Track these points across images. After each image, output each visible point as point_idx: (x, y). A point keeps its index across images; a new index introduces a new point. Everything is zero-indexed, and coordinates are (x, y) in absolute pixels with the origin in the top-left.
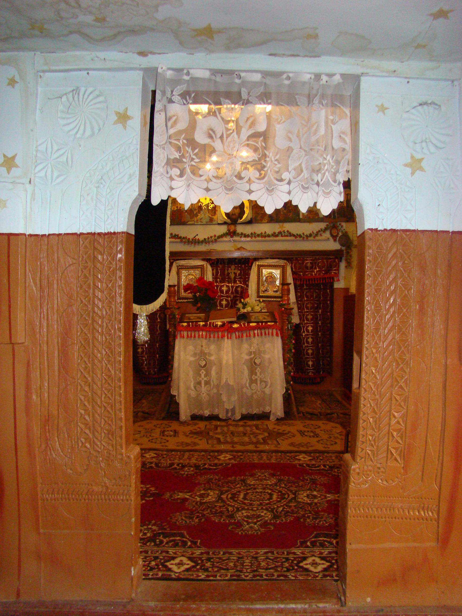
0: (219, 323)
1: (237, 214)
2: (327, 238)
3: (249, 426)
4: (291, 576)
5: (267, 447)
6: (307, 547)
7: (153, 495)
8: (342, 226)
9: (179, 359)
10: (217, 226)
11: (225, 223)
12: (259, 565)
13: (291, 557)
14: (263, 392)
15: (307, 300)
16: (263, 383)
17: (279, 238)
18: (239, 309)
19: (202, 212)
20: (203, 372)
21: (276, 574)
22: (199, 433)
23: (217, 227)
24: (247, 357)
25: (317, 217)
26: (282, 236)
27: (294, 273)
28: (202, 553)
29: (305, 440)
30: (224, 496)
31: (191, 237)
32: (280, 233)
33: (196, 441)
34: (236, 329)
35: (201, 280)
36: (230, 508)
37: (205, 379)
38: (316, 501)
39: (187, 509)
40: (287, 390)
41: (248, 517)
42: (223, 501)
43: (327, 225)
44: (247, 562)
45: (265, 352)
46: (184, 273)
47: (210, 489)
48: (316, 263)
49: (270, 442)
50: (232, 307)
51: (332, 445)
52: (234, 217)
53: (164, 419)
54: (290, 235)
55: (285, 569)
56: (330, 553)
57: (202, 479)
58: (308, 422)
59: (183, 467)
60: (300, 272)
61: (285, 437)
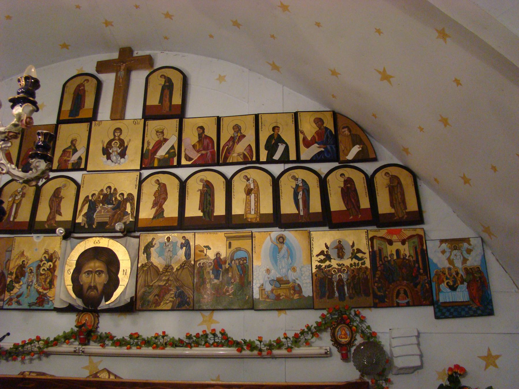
1: (100, 288)
2: (323, 351)
8: (363, 320)
10: (54, 314)
11: (70, 309)
19: (23, 280)
23: (54, 315)
25: (296, 297)
26: (207, 345)
43: (323, 316)
52: (93, 293)
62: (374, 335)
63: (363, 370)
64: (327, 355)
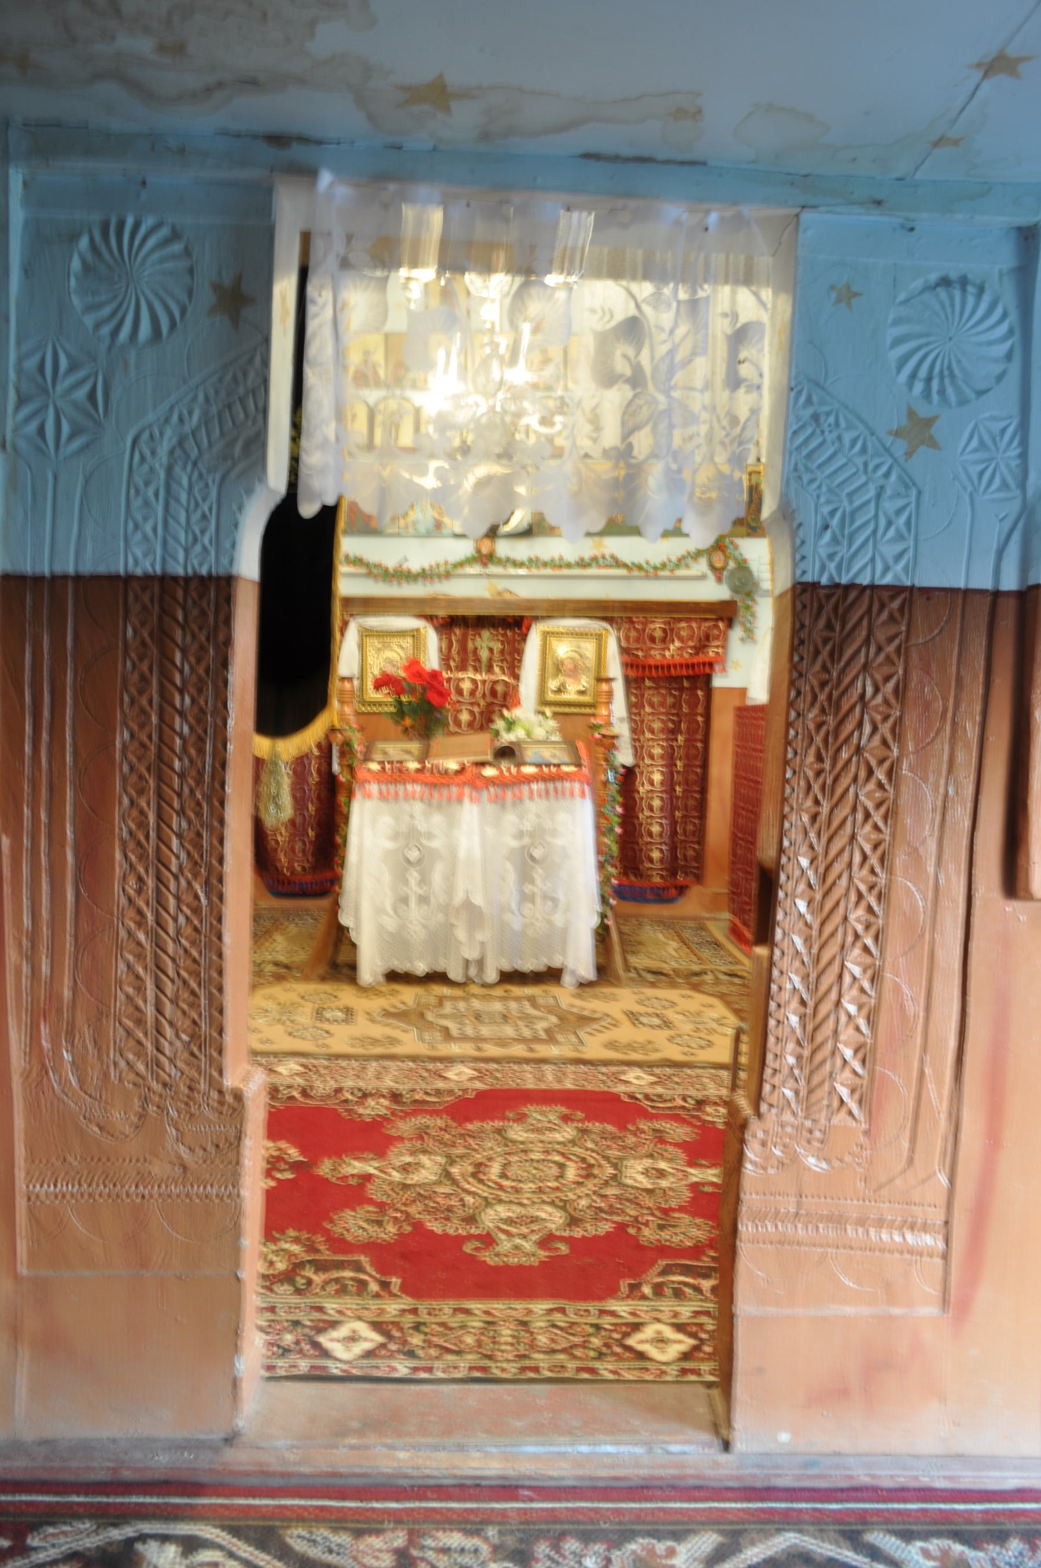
0: (452, 765)
2: (700, 574)
3: (517, 999)
4: (605, 1369)
5: (554, 1051)
6: (644, 1297)
7: (295, 1166)
8: (736, 547)
9: (361, 847)
12: (532, 1345)
13: (607, 1321)
14: (550, 922)
15: (652, 714)
16: (550, 903)
17: (593, 571)
18: (497, 733)
20: (414, 876)
21: (572, 1365)
22: (401, 1015)
24: (514, 843)
26: (599, 566)
27: (624, 651)
28: (403, 1311)
29: (640, 1035)
30: (455, 1170)
31: (391, 563)
32: (594, 559)
33: (396, 1034)
34: (490, 781)
35: (413, 666)
36: (469, 1200)
37: (420, 892)
38: (664, 1183)
39: (371, 1201)
40: (603, 916)
41: (510, 1221)
42: (455, 1182)
44: (506, 1333)
45: (554, 833)
46: (373, 643)
47: (425, 1152)
48: (672, 630)
49: (560, 1037)
50: (482, 728)
51: (702, 1048)
53: (323, 979)
54: (618, 563)
55: (592, 1354)
56: (697, 1313)
57: (405, 1127)
58: (650, 992)
59: (365, 1095)
60: (637, 649)
61: (596, 1026)
62: (745, 561)
63: (735, 590)
64: (703, 577)
